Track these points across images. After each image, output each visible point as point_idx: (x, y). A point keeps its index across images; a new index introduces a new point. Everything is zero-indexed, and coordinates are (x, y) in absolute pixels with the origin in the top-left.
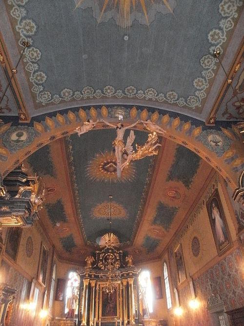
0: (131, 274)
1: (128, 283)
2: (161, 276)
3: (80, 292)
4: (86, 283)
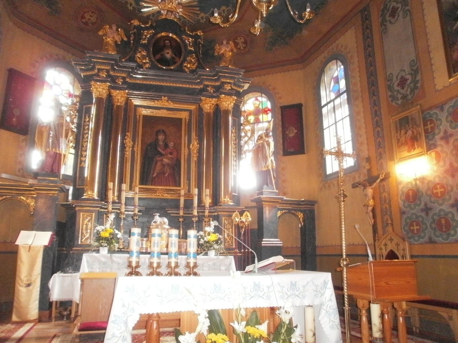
0: (228, 87)
1: (217, 107)
2: (303, 103)
3: (80, 118)
4: (99, 90)
